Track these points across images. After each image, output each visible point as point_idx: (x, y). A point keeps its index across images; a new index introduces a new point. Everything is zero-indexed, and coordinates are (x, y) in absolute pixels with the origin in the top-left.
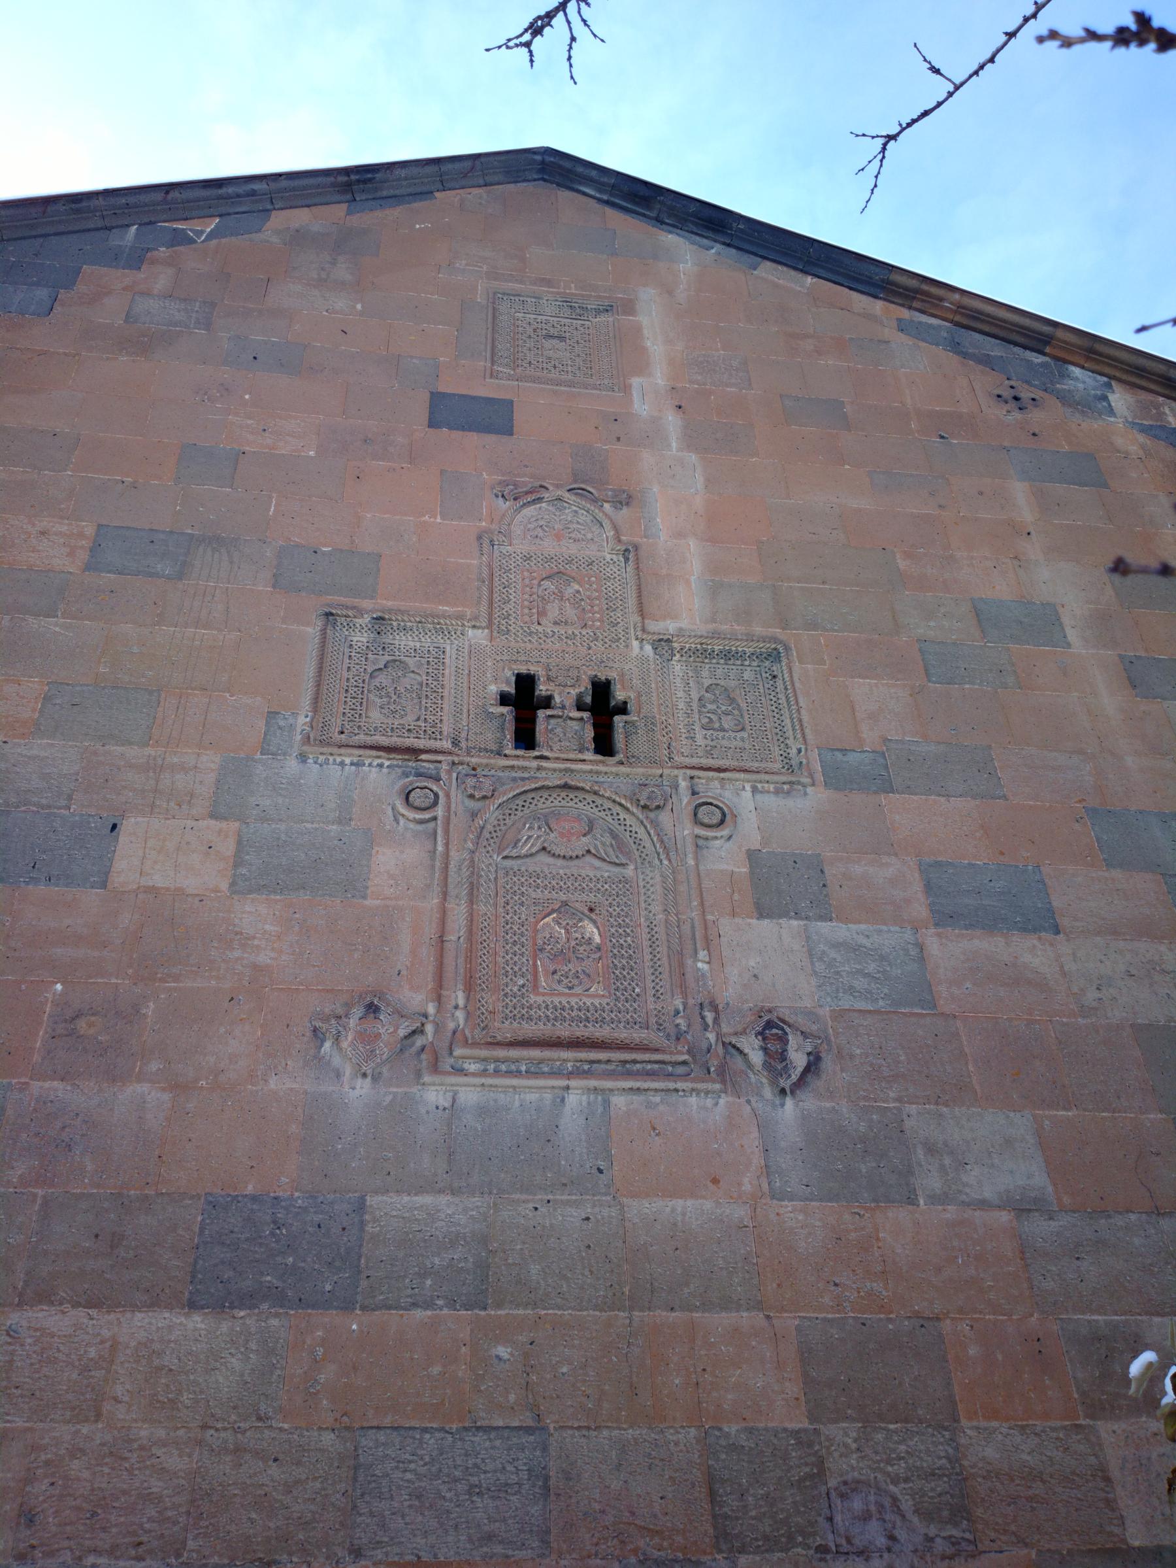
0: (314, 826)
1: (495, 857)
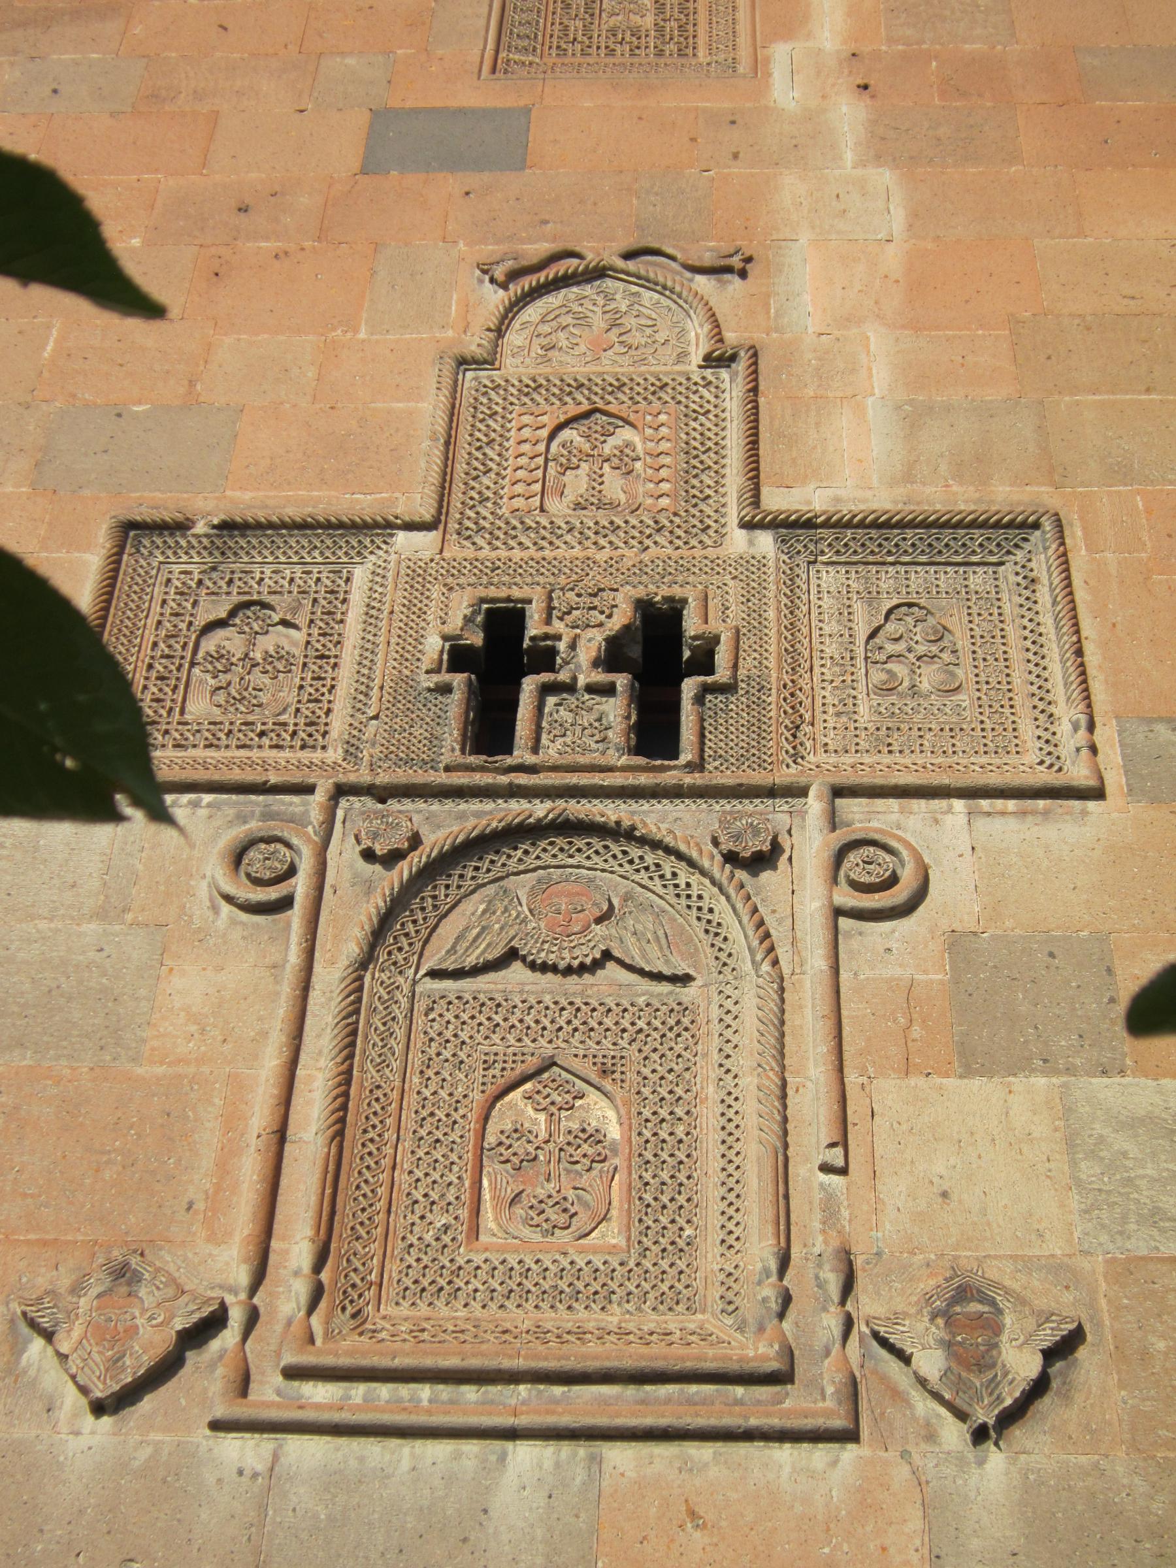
0: (52, 925)
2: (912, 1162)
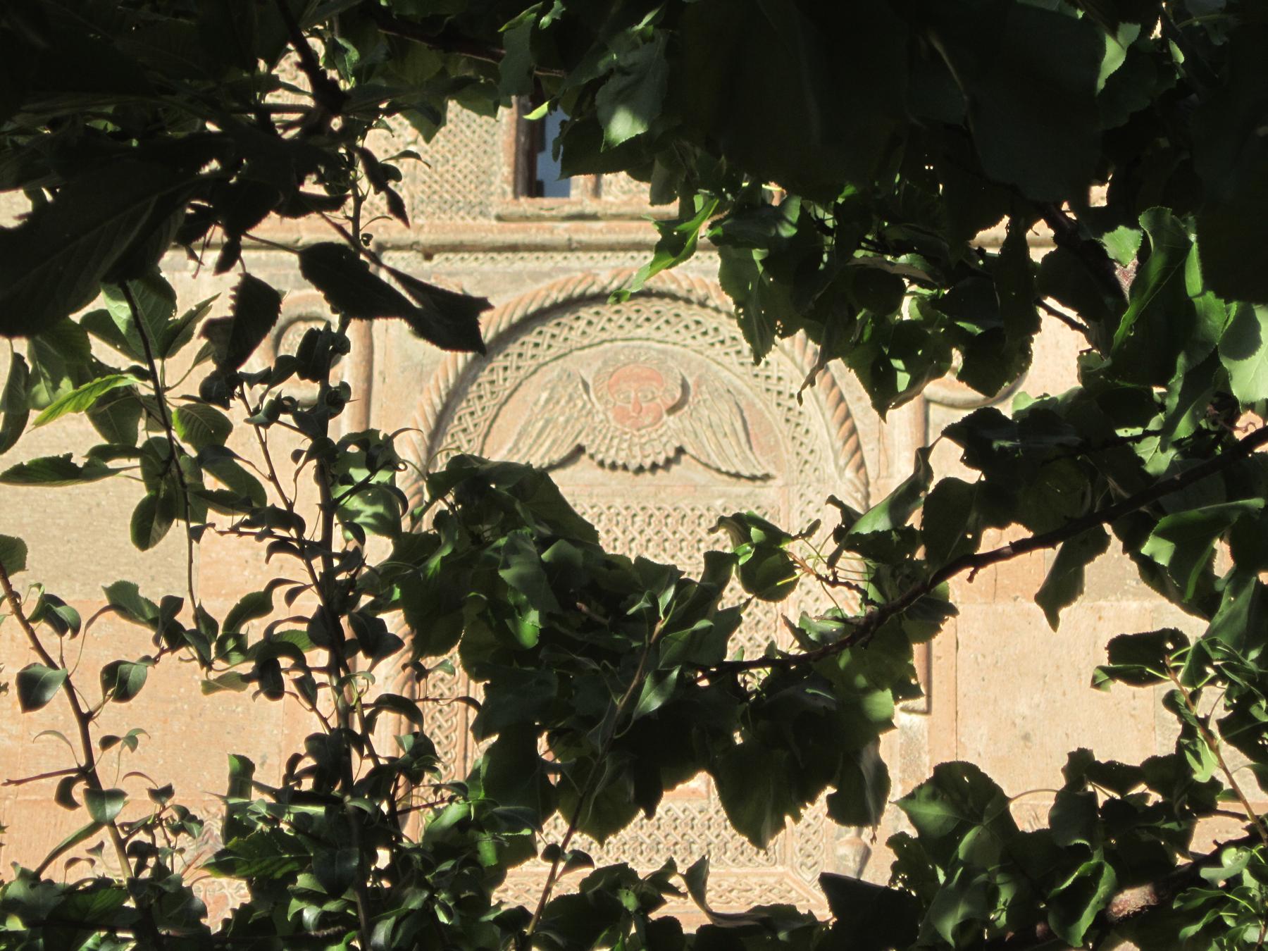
2: (995, 700)
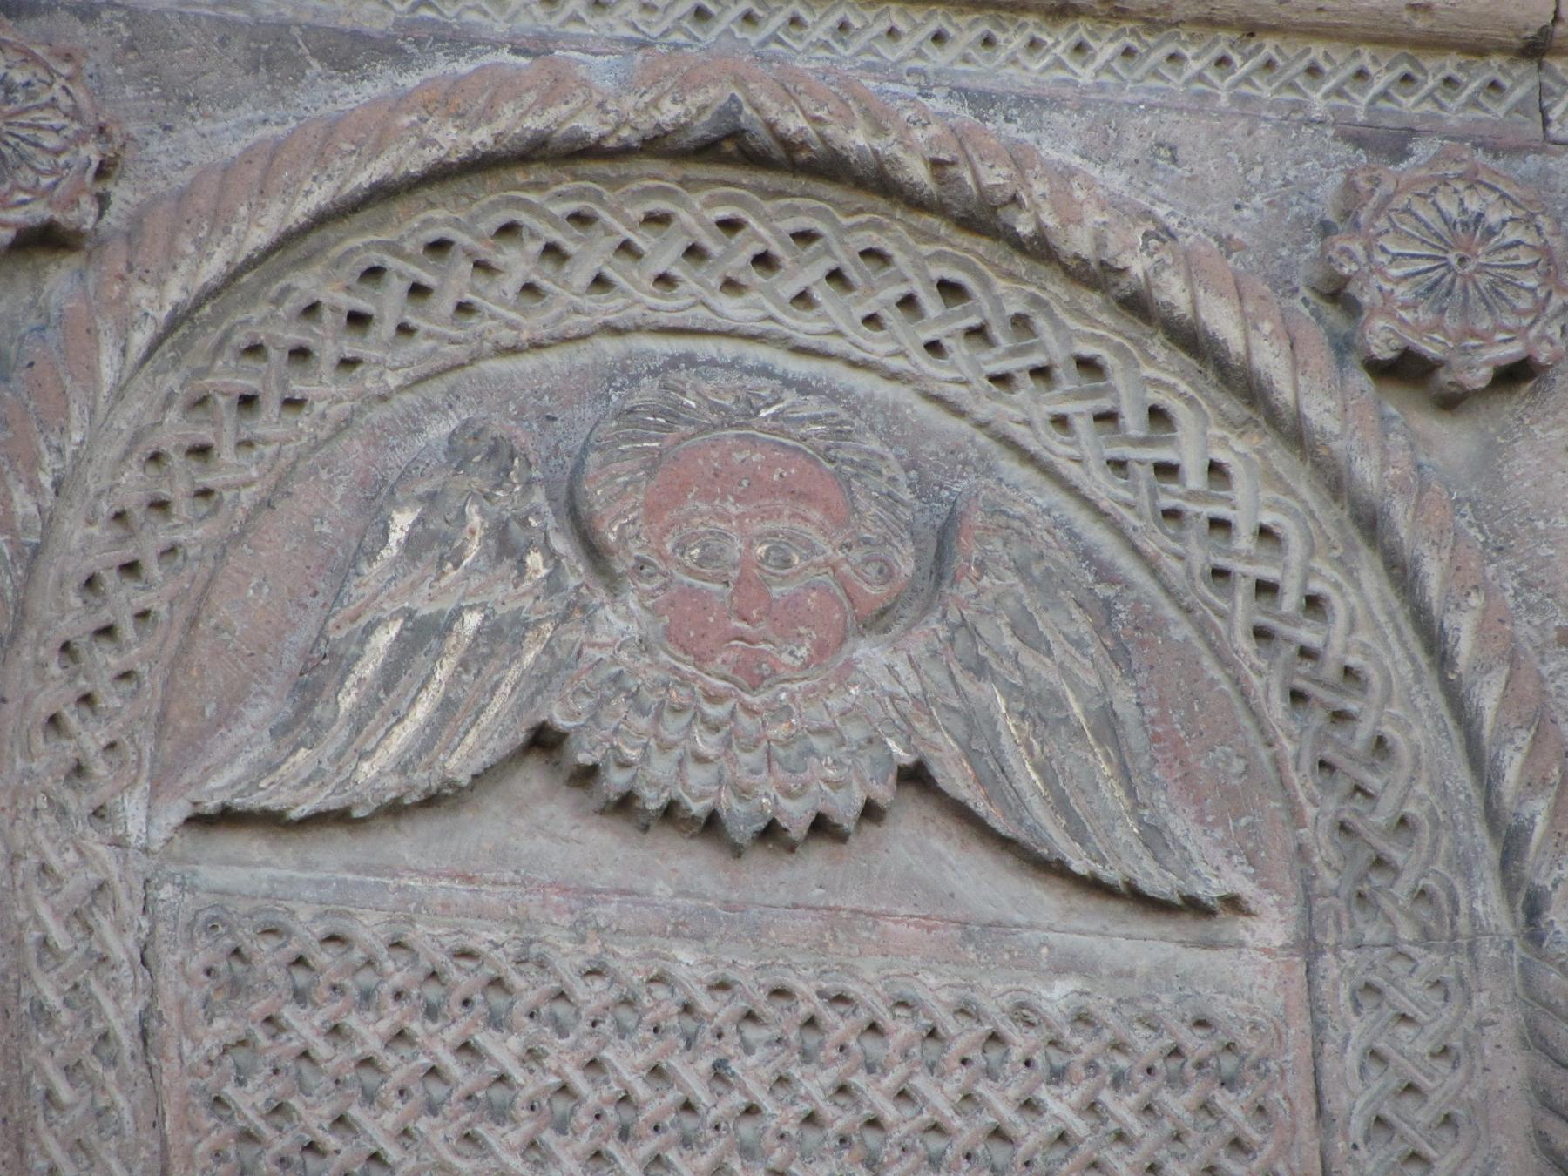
1: (133, 813)
